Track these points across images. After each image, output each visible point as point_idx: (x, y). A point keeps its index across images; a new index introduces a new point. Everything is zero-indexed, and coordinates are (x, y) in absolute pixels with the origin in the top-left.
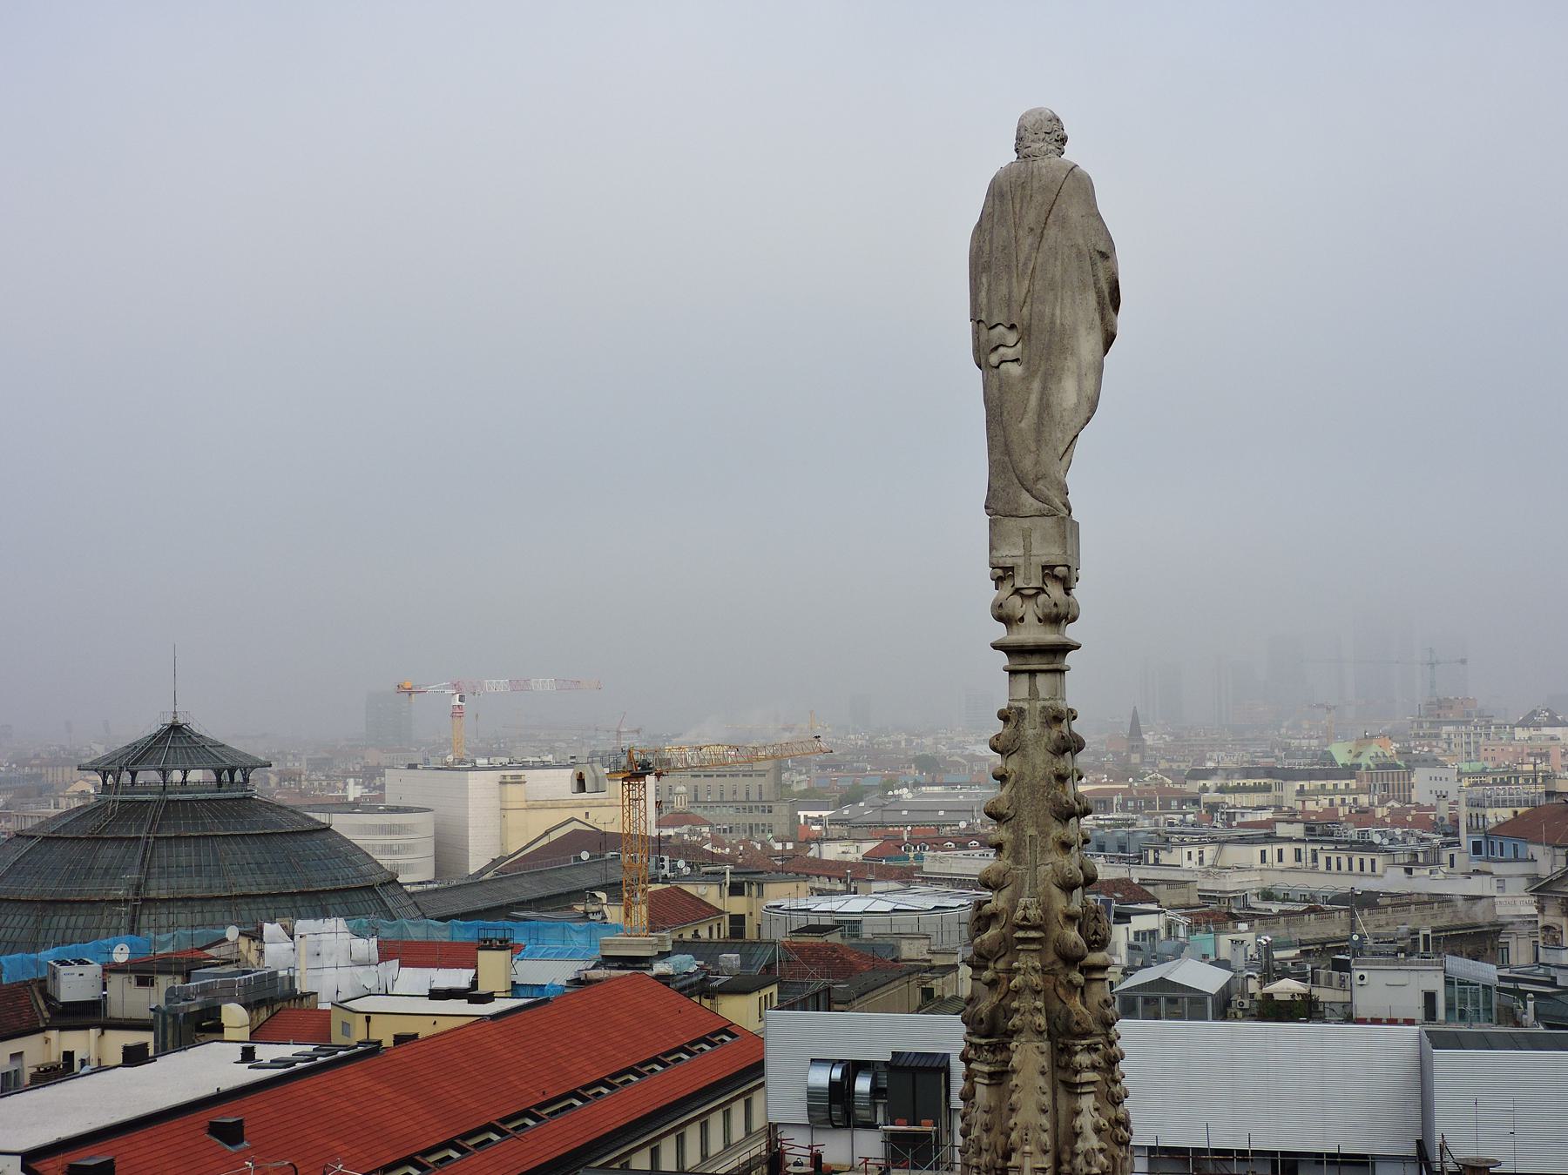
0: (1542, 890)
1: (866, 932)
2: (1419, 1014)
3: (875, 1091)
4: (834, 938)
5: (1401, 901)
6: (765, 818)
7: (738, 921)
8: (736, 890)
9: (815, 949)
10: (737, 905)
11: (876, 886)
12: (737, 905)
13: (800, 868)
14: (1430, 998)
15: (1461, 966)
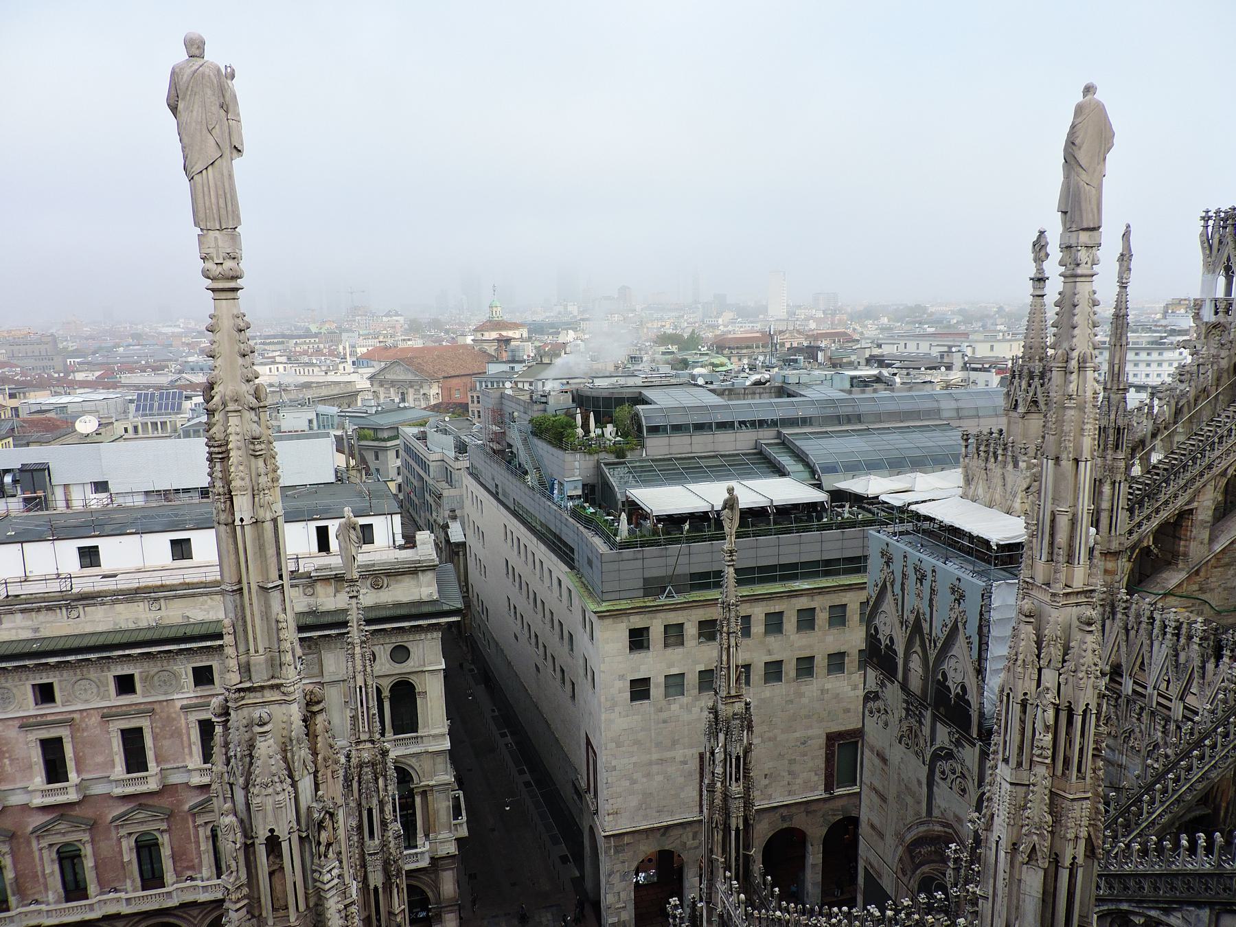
0: (371, 378)
1: (69, 411)
2: (307, 428)
3: (15, 481)
4: (48, 415)
5: (319, 385)
6: (51, 363)
7: (16, 409)
8: (12, 396)
9: (40, 420)
10: (14, 403)
11: (78, 391)
12: (14, 403)
13: (41, 385)
14: (310, 421)
15: (322, 409)
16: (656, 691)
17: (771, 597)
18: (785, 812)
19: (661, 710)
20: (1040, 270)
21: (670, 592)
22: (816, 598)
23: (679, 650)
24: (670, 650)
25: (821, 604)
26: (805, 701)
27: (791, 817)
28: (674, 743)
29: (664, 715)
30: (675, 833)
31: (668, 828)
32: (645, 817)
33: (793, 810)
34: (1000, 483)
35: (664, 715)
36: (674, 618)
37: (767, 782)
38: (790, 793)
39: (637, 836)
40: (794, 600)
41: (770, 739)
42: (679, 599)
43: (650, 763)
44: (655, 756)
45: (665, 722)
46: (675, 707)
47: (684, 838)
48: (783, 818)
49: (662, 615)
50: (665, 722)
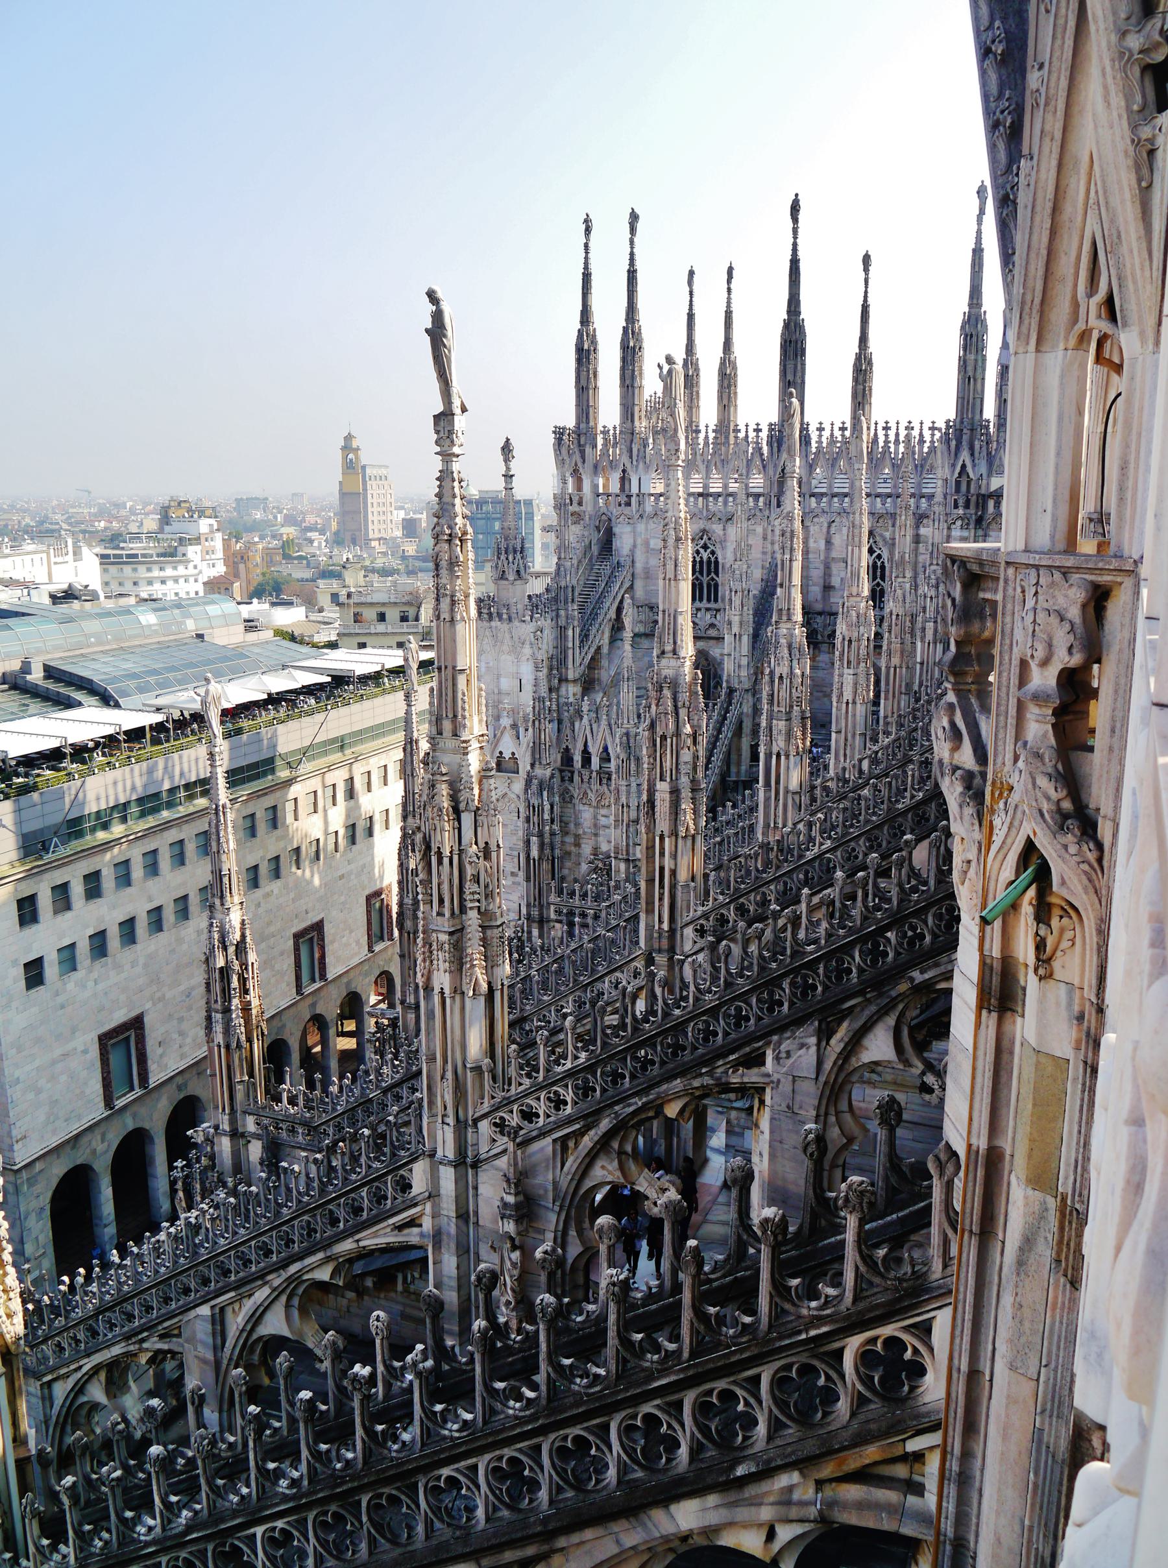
16: (51, 971)
17: (167, 826)
18: (179, 1080)
19: (57, 994)
20: (508, 469)
21: (56, 846)
22: (185, 827)
23: (68, 915)
24: (60, 917)
25: (188, 833)
26: (185, 947)
27: (185, 1085)
28: (74, 1030)
29: (60, 999)
30: (84, 1140)
31: (77, 1137)
32: (54, 1132)
33: (187, 1075)
34: (507, 635)
35: (60, 999)
36: (58, 877)
37: (160, 1051)
38: (183, 1056)
39: (48, 1159)
40: (166, 834)
41: (160, 1000)
42: (63, 851)
43: (54, 1062)
44: (58, 1052)
45: (62, 1007)
46: (70, 986)
47: (94, 1143)
48: (179, 1088)
49: (47, 876)
50: (62, 1007)
